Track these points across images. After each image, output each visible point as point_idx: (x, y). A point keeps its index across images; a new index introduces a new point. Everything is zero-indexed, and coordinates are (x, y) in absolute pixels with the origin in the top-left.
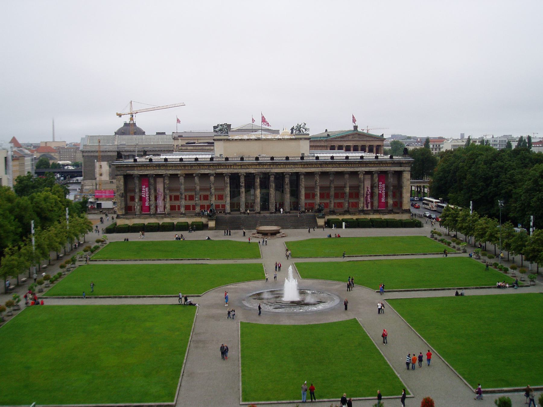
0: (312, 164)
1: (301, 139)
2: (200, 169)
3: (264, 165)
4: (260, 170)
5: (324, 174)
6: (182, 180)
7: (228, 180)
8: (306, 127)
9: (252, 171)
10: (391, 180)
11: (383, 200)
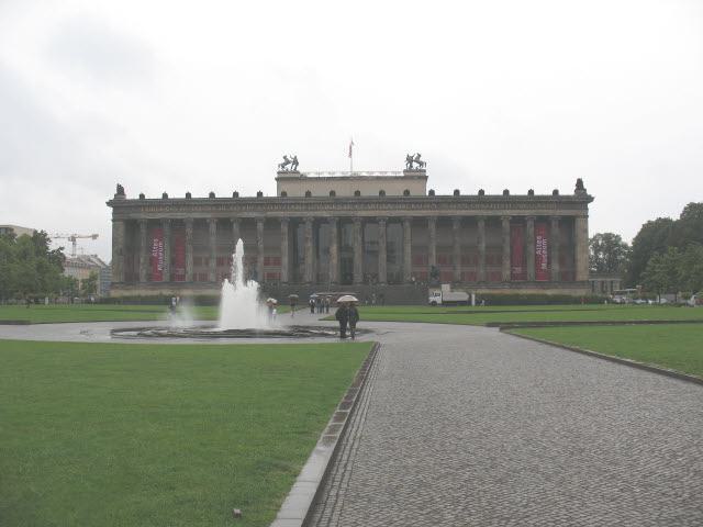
0: (423, 203)
1: (412, 178)
2: (241, 211)
3: (343, 204)
4: (337, 213)
5: (444, 222)
6: (213, 228)
7: (285, 229)
8: (421, 159)
9: (325, 214)
10: (556, 231)
11: (544, 266)
